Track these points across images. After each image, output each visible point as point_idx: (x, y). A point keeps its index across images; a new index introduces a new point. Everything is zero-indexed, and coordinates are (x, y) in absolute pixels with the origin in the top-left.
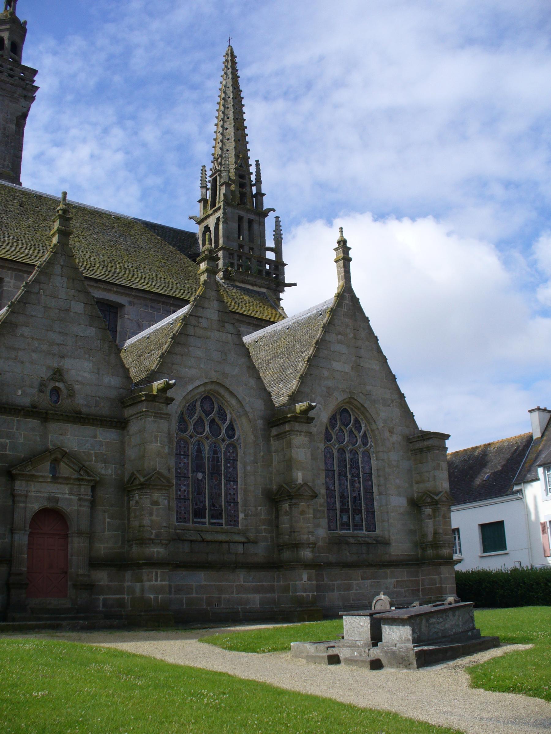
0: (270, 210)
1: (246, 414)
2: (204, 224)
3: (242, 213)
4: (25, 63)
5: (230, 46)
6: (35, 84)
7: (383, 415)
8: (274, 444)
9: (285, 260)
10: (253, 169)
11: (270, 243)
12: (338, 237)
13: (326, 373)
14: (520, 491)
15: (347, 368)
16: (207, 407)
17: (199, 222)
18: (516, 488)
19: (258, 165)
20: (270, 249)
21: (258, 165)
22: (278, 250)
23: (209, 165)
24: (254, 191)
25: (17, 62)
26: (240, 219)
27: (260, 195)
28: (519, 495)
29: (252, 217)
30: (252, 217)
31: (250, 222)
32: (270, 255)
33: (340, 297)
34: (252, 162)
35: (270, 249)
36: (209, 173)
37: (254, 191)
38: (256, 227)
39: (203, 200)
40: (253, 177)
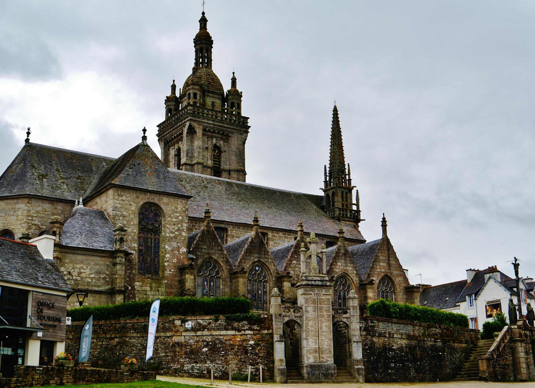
0: (354, 187)
1: (353, 282)
2: (328, 192)
3: (343, 190)
4: (243, 115)
5: (335, 106)
6: (249, 125)
7: (398, 280)
8: (362, 291)
9: (360, 209)
10: (347, 167)
11: (354, 201)
12: (382, 217)
13: (378, 267)
14: (459, 306)
15: (385, 265)
16: (342, 280)
17: (324, 191)
18: (457, 304)
19: (349, 166)
20: (354, 204)
21: (349, 166)
22: (357, 205)
23: (328, 166)
24: (347, 178)
25: (239, 113)
26: (342, 192)
27: (350, 180)
28: (458, 307)
29: (347, 191)
30: (347, 191)
31: (346, 193)
32: (354, 208)
33: (383, 239)
34: (346, 163)
35: (354, 204)
36: (328, 169)
37: (347, 178)
38: (349, 195)
39: (326, 182)
40: (347, 171)
